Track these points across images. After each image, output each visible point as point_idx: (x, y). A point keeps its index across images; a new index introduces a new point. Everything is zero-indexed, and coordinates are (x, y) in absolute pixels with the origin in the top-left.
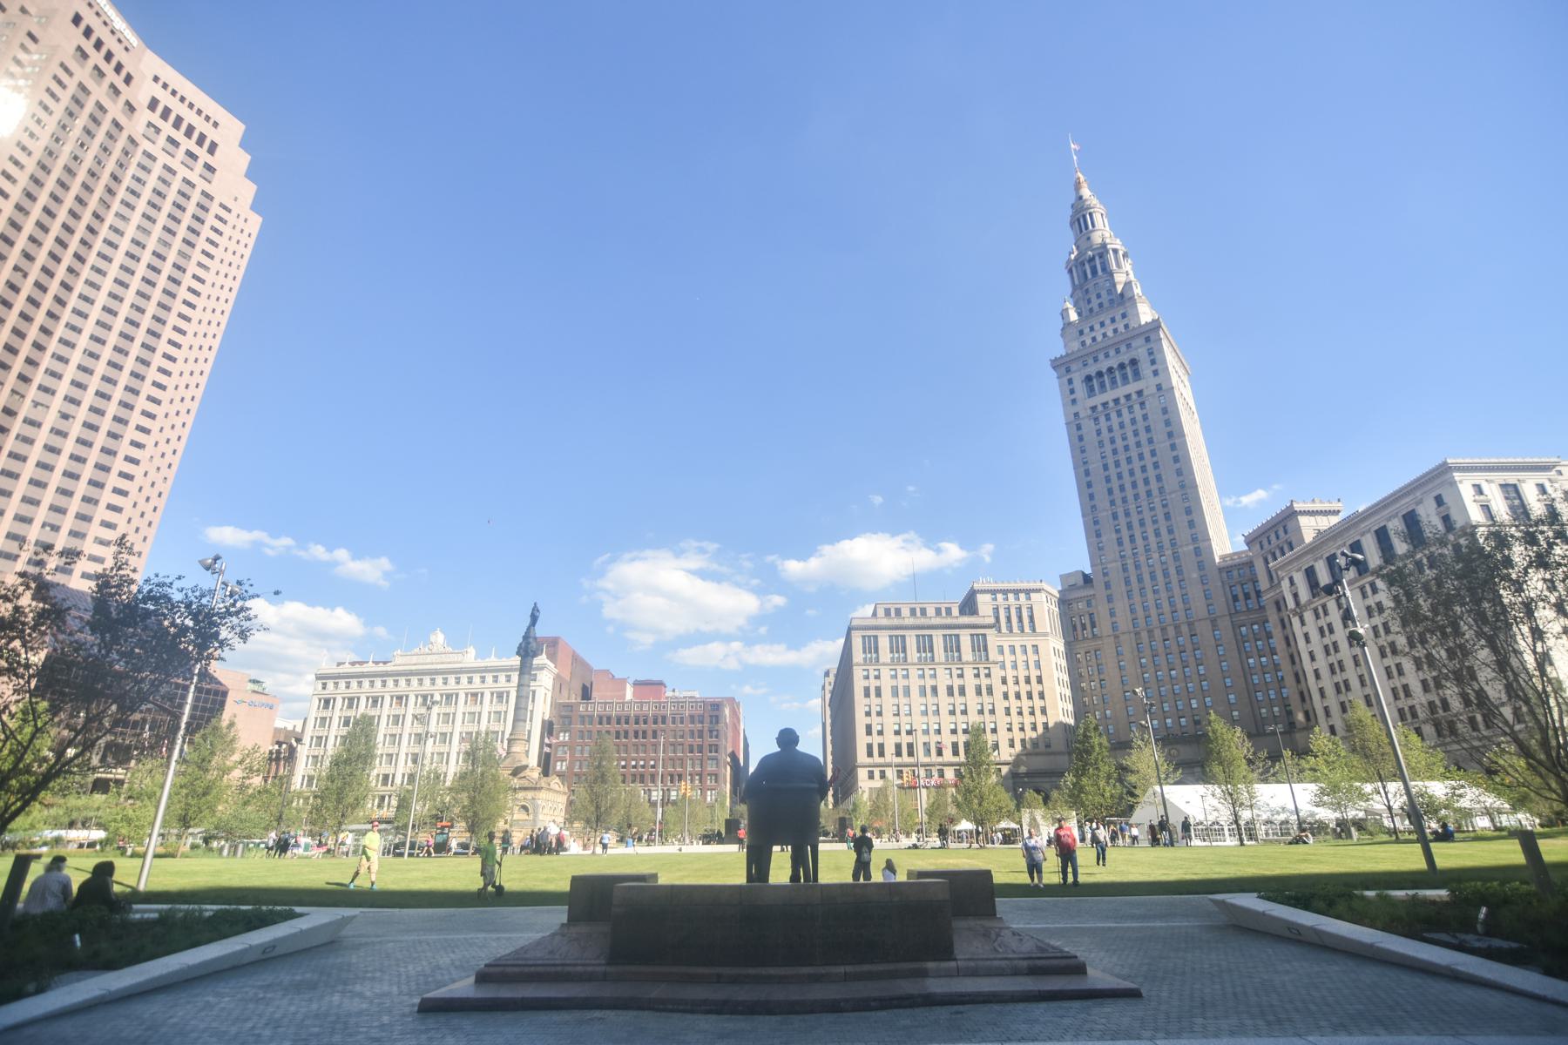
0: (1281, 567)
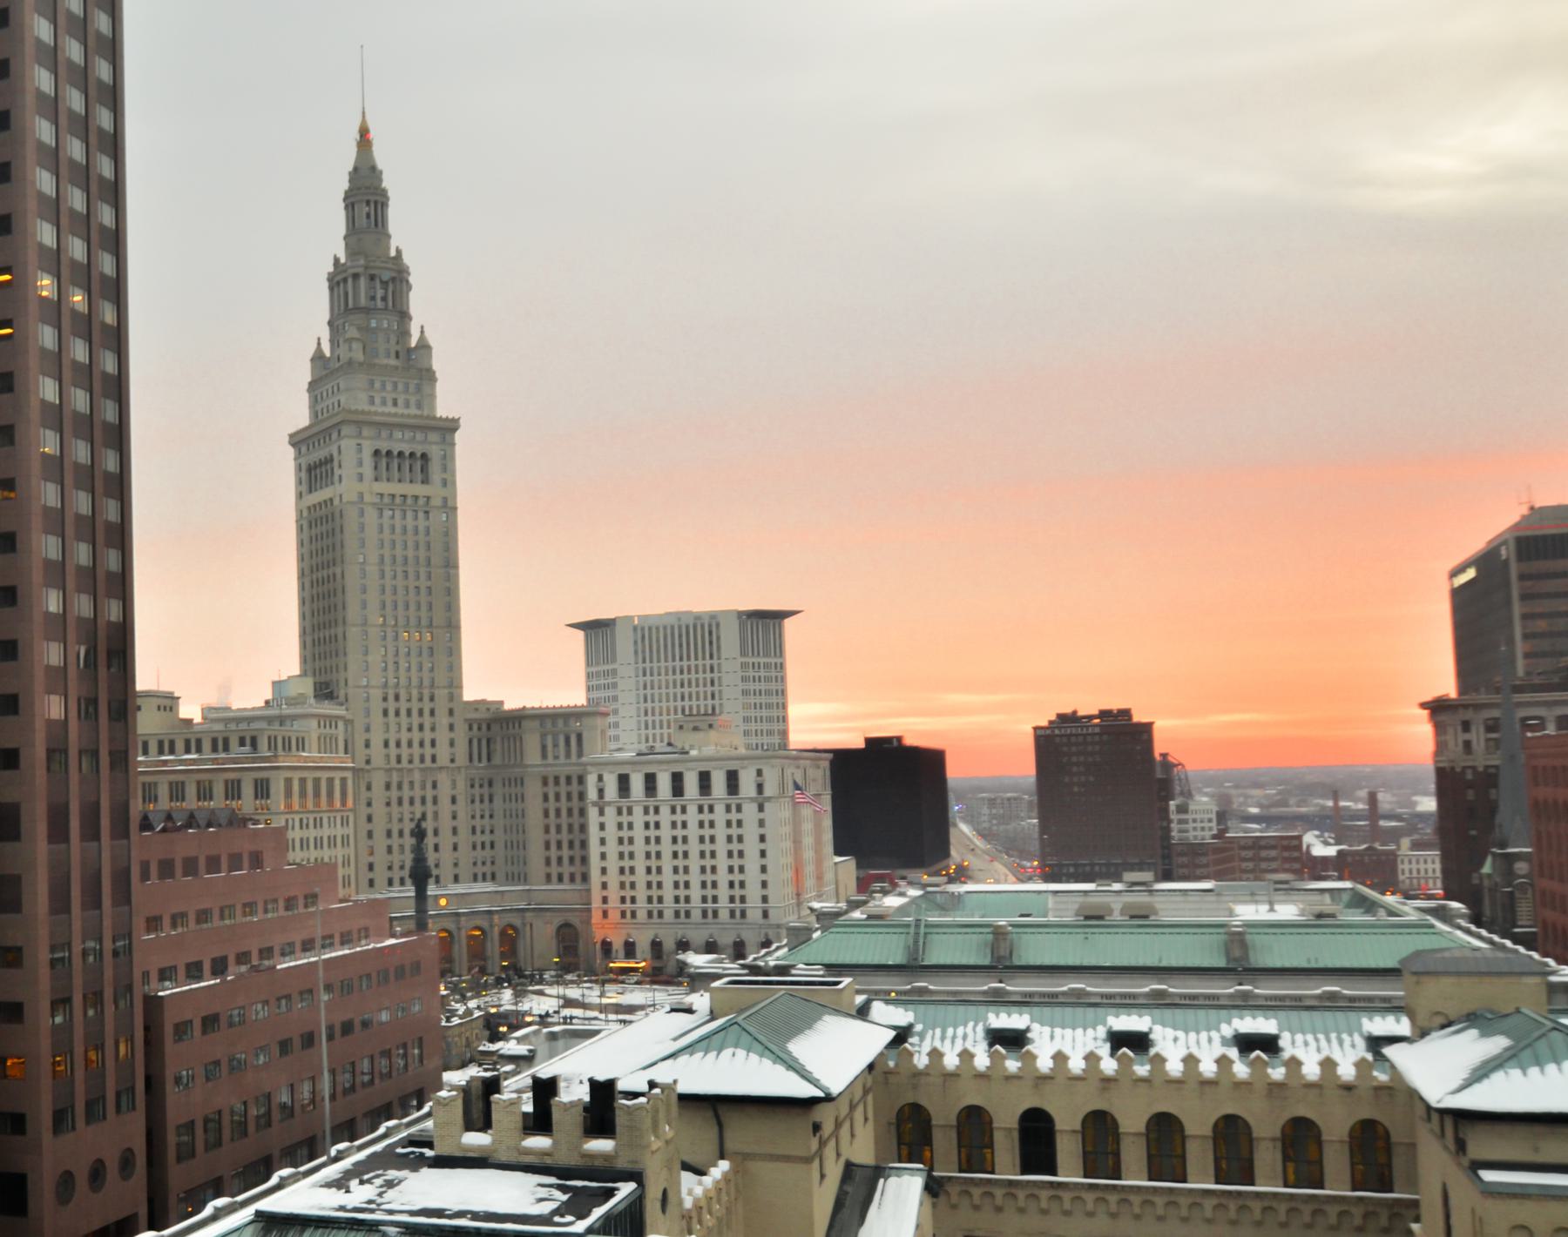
0: (593, 765)
